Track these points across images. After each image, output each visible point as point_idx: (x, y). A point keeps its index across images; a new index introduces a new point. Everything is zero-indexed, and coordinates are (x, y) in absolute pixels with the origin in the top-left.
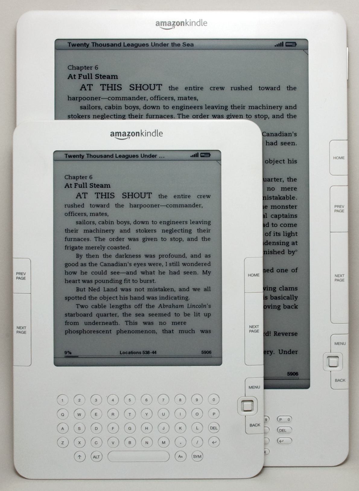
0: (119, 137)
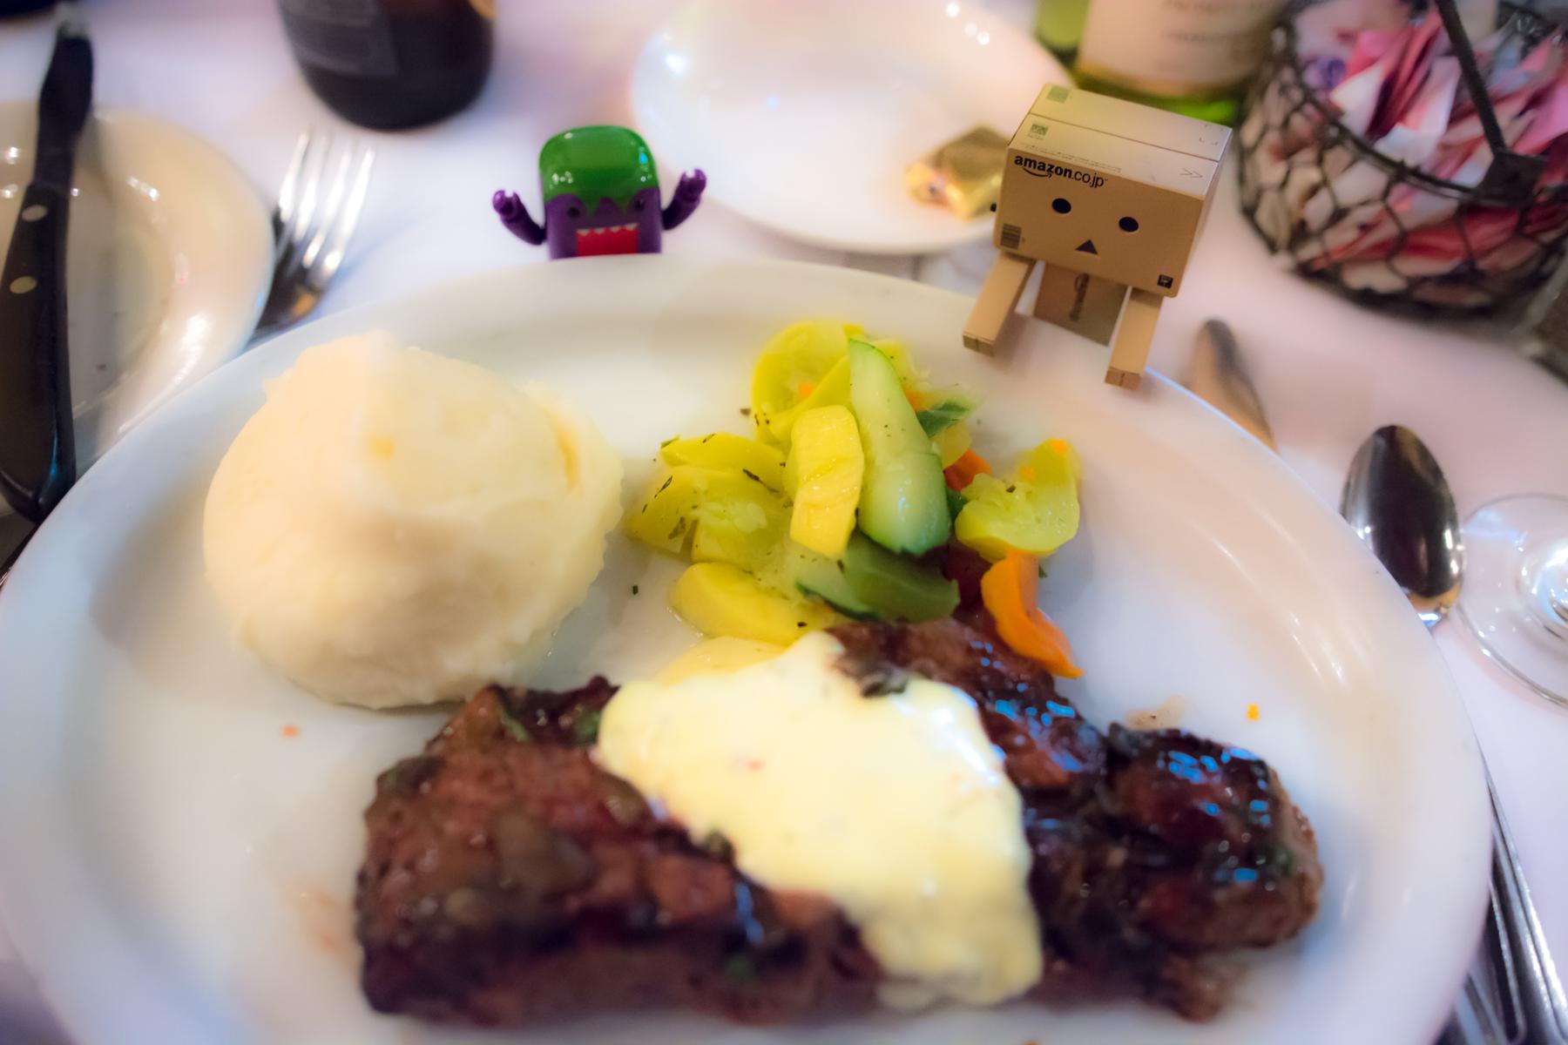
0: (1031, 169)
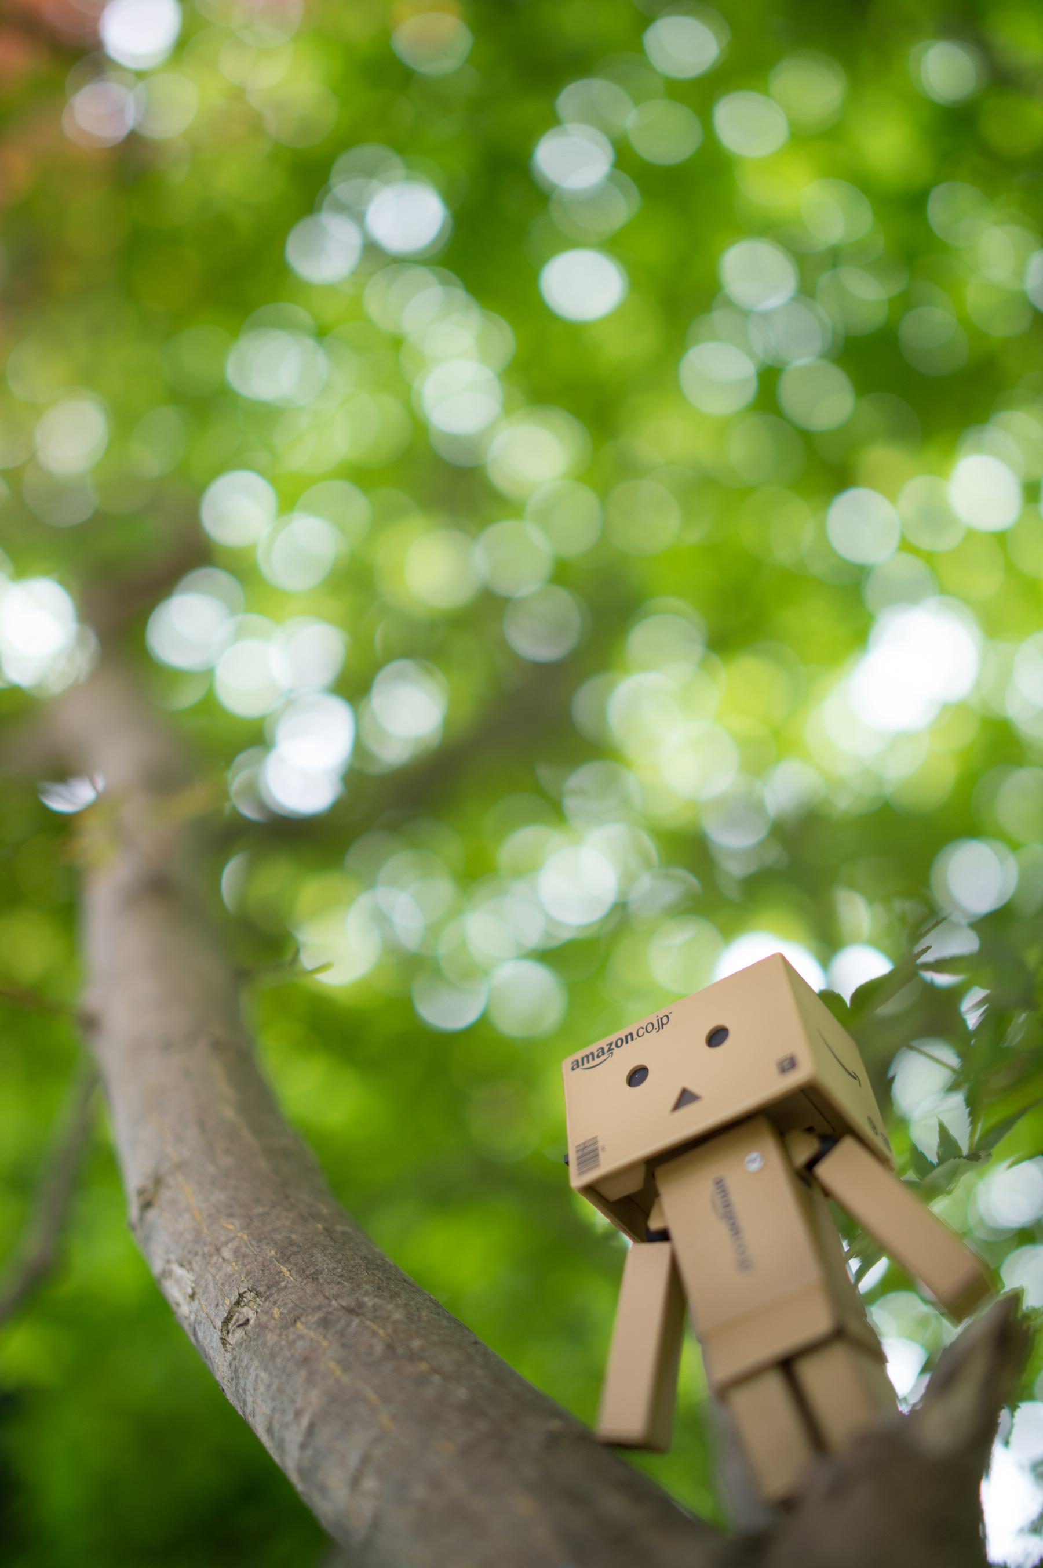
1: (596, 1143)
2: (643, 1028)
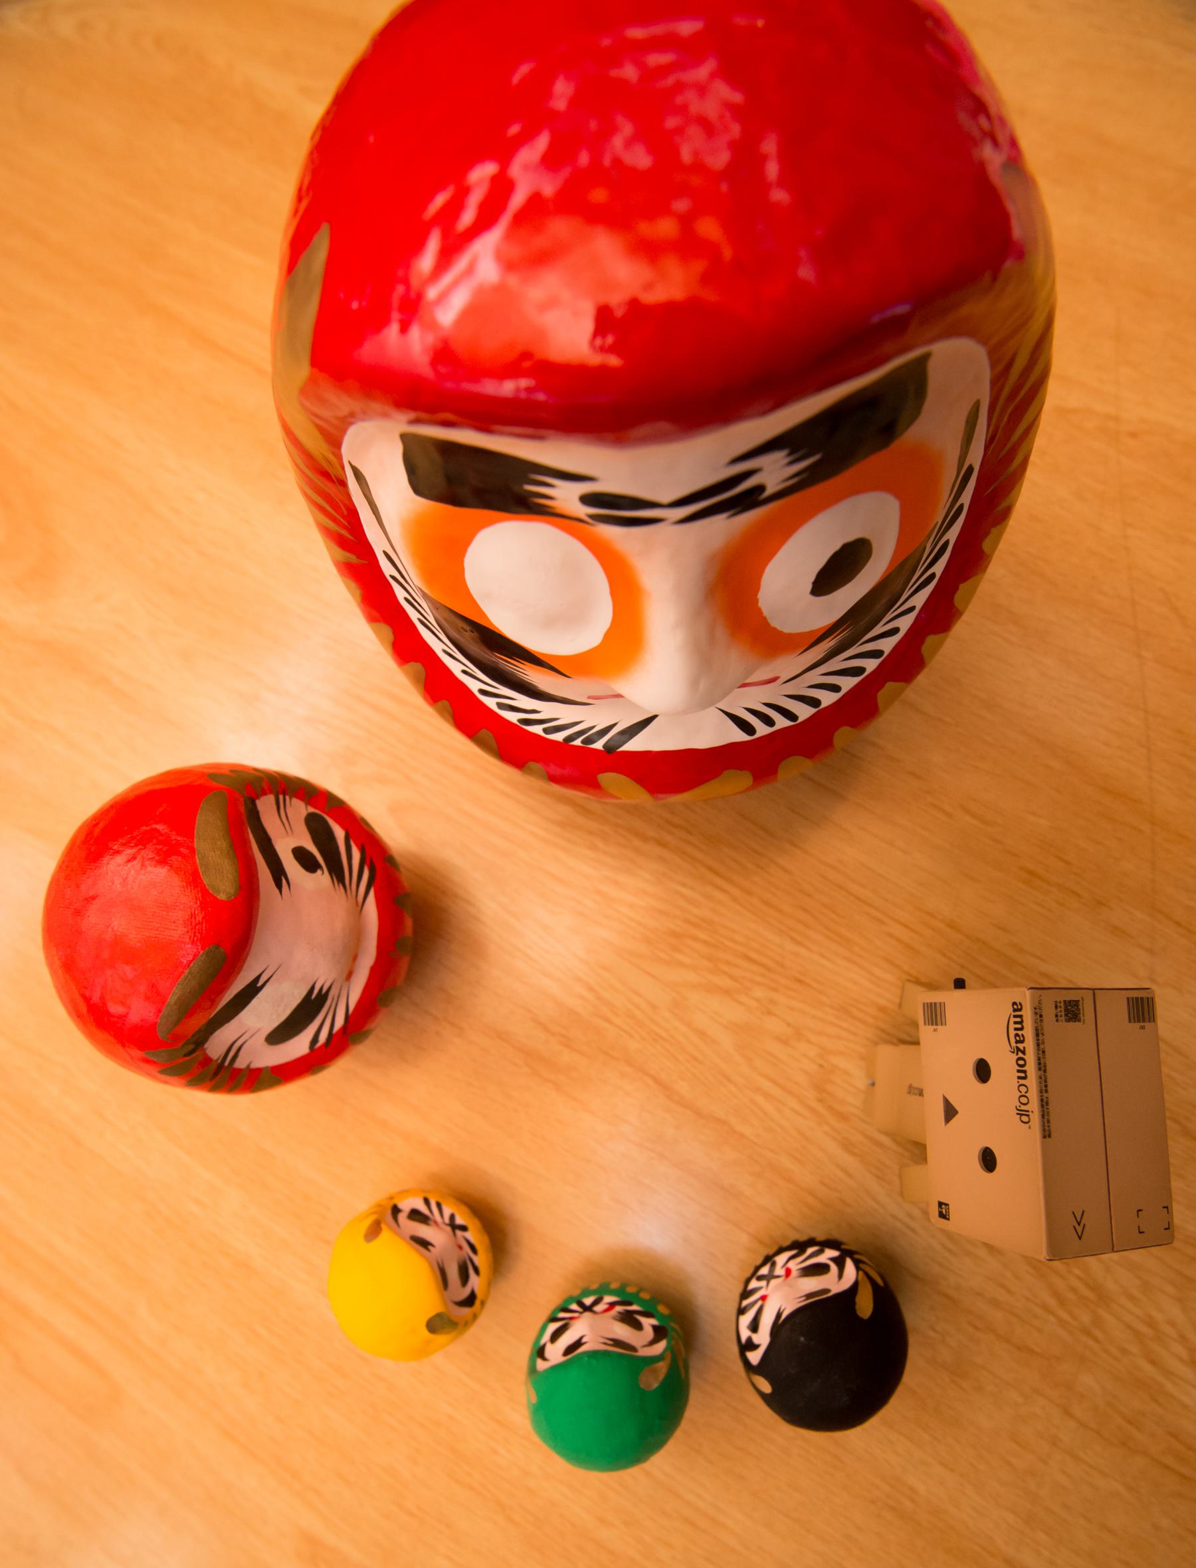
0: (1012, 1026)
1: (942, 1024)
2: (1026, 1092)
